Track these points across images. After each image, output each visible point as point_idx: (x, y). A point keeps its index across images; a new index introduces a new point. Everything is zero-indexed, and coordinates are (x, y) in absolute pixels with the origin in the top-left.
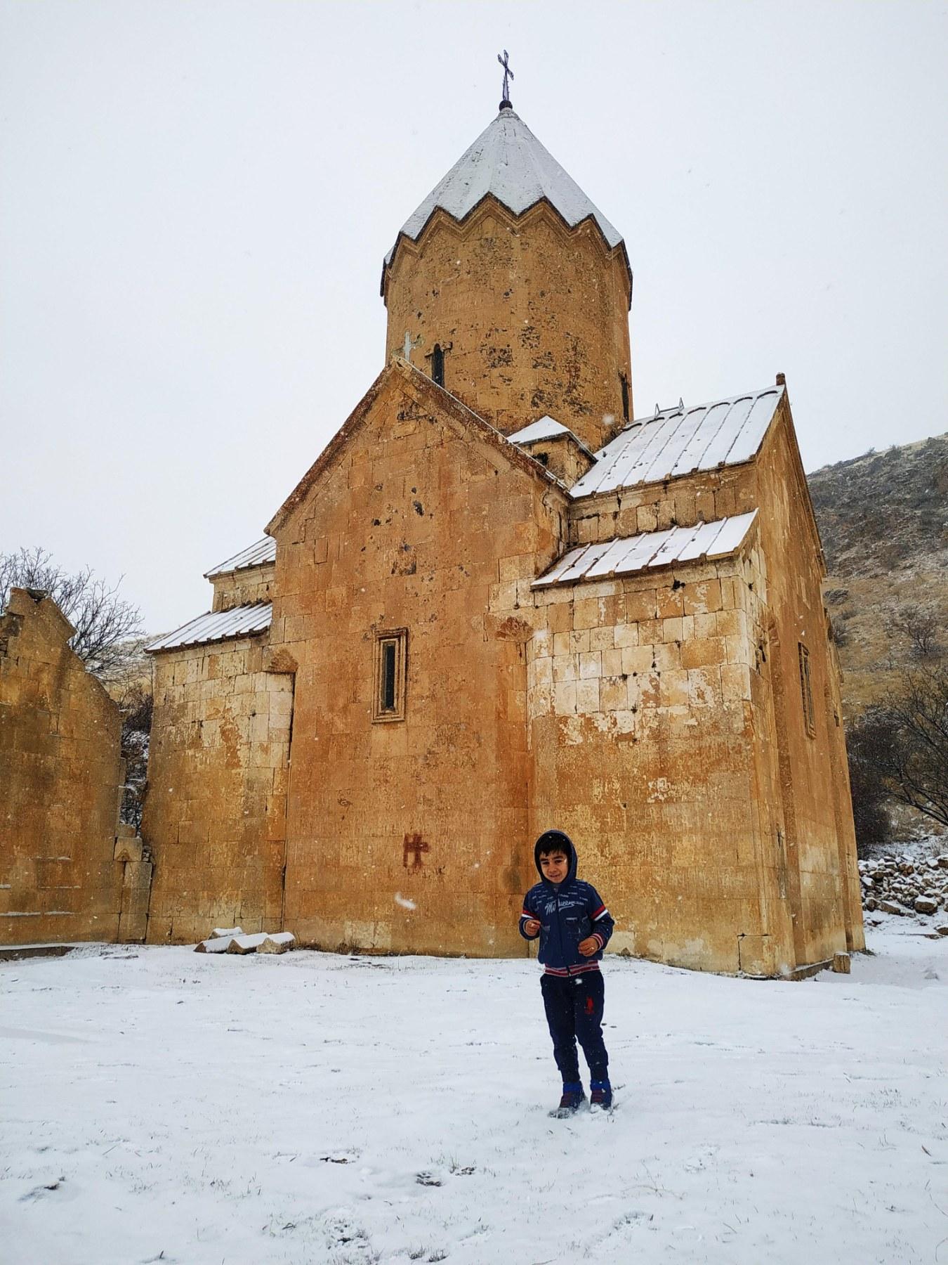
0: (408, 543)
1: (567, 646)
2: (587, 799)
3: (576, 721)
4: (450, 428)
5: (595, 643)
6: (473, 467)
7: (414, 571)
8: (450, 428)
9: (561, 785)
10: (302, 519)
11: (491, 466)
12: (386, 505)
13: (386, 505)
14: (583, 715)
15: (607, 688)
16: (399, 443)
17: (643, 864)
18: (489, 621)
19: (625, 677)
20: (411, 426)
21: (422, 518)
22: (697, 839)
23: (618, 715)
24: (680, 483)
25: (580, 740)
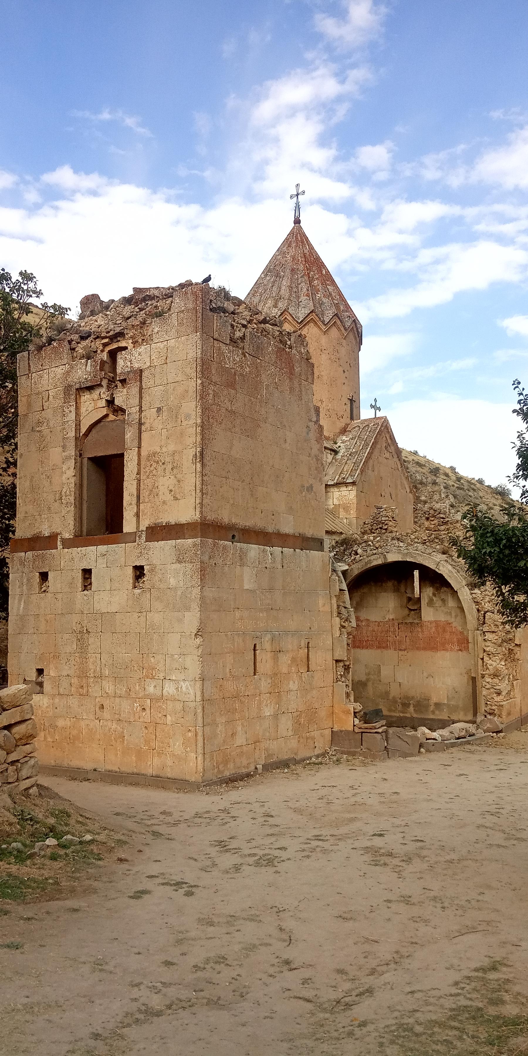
20: (387, 455)
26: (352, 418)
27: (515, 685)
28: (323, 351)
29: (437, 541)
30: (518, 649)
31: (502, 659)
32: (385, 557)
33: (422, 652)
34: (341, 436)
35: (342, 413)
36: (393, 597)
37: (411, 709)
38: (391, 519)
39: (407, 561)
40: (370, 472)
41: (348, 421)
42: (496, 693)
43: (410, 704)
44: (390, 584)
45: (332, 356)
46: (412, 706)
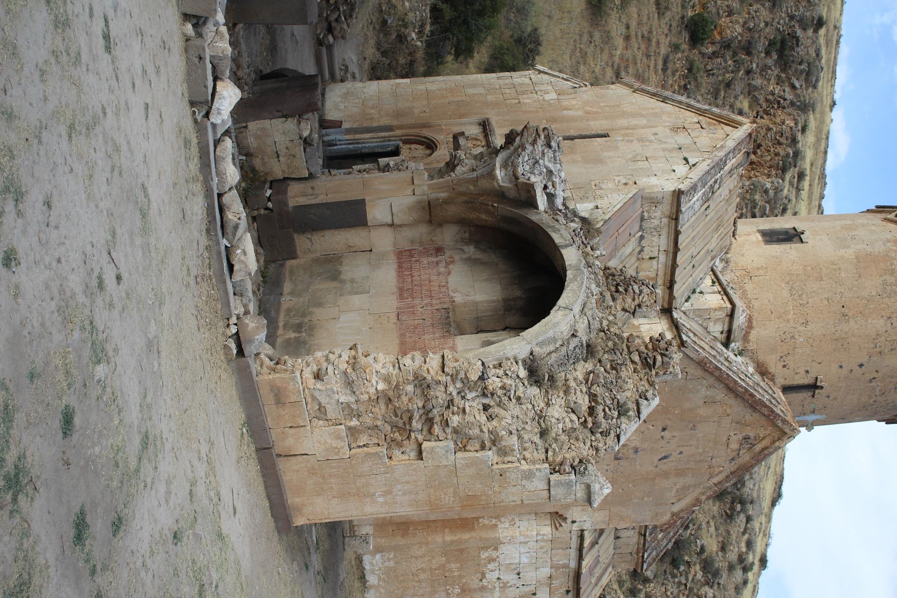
1: (542, 548)
2: (448, 562)
3: (494, 554)
4: (720, 472)
5: (541, 560)
6: (685, 488)
7: (616, 459)
8: (720, 472)
9: (457, 550)
10: (686, 370)
11: (679, 500)
12: (675, 434)
13: (675, 434)
14: (498, 557)
15: (513, 567)
16: (725, 438)
17: (414, 586)
18: (568, 507)
19: (518, 574)
20: (734, 446)
21: (656, 460)
23: (497, 572)
24: (642, 541)
25: (483, 557)
26: (786, 389)
27: (340, 427)
28: (889, 321)
29: (610, 344)
30: (413, 455)
31: (389, 383)
32: (567, 246)
33: (397, 341)
34: (752, 365)
35: (791, 365)
36: (495, 298)
38: (637, 302)
39: (565, 271)
41: (780, 381)
42: (319, 370)
43: (300, 332)
44: (518, 293)
45: (883, 338)
46: (297, 335)
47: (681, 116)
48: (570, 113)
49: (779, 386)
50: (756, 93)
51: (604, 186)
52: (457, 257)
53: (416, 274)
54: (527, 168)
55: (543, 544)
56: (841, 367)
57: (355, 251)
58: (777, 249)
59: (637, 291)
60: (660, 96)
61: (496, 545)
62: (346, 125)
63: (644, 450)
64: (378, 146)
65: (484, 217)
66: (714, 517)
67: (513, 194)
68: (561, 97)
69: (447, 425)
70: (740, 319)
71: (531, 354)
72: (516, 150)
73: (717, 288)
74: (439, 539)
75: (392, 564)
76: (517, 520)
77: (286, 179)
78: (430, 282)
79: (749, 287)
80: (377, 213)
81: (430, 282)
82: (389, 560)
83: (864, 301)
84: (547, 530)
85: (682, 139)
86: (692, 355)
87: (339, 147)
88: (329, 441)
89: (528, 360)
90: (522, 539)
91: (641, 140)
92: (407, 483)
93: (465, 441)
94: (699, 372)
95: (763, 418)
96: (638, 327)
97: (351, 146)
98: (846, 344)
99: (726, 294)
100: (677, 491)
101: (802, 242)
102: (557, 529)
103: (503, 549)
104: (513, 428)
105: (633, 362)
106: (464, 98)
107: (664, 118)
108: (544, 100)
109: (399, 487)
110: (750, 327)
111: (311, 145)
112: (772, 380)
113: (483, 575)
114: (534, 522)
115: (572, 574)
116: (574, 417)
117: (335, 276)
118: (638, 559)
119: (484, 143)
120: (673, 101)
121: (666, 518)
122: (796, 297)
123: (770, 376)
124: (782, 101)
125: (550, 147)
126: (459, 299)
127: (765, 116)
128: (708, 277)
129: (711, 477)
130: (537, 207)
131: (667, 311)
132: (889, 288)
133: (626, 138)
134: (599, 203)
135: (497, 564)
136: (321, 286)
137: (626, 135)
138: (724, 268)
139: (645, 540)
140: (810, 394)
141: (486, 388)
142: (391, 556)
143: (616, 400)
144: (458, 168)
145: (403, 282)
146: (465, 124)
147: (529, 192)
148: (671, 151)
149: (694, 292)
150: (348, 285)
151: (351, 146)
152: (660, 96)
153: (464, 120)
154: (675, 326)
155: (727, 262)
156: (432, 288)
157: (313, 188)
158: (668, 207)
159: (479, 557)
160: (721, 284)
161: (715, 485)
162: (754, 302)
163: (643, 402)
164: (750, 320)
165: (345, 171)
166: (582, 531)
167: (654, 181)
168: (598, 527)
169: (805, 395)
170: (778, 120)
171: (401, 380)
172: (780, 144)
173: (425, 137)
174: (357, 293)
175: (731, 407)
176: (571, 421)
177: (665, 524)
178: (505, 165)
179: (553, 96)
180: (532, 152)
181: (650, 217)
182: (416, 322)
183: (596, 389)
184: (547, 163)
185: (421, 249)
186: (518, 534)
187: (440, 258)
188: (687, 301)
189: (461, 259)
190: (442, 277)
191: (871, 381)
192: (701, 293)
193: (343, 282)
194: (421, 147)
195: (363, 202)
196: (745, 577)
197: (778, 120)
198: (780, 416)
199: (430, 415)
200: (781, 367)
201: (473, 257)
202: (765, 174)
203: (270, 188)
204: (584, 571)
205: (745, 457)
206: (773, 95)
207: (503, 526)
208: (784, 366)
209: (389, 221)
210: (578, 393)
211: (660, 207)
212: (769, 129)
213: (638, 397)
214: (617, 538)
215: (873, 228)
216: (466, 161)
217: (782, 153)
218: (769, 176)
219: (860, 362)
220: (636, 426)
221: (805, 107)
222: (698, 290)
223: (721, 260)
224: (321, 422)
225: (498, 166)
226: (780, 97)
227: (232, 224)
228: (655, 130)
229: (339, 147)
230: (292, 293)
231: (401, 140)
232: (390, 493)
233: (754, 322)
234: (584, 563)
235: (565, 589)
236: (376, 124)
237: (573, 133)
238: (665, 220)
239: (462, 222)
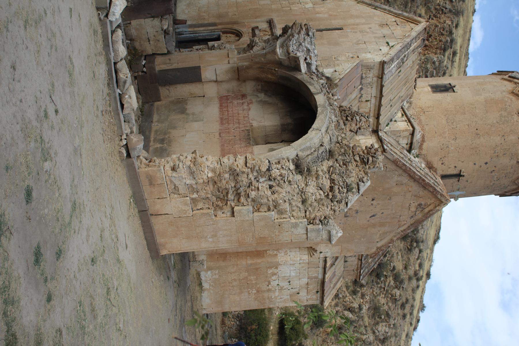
0: (359, 214)
1: (303, 267)
3: (276, 271)
4: (405, 224)
5: (302, 274)
6: (385, 233)
7: (346, 216)
8: (405, 224)
10: (386, 166)
11: (381, 240)
15: (286, 278)
16: (408, 205)
17: (230, 289)
18: (317, 244)
19: (289, 282)
20: (413, 209)
22: (238, 299)
23: (277, 281)
24: (360, 264)
25: (269, 272)
26: (443, 177)
28: (503, 138)
29: (343, 150)
30: (229, 214)
31: (215, 173)
32: (318, 93)
34: (424, 163)
35: (446, 163)
36: (276, 124)
37: (159, 145)
38: (358, 126)
40: (396, 178)
41: (440, 172)
43: (163, 144)
44: (289, 121)
46: (161, 145)
47: (385, 18)
48: (321, 15)
49: (439, 175)
50: (429, 5)
51: (340, 59)
52: (254, 100)
53: (230, 110)
54: (295, 48)
55: (303, 265)
56: (475, 164)
57: (194, 96)
58: (439, 96)
59: (358, 120)
60: (373, 6)
61: (276, 266)
62: (189, 23)
63: (361, 211)
64: (208, 35)
65: (270, 76)
66: (401, 250)
67: (286, 63)
68: (315, 6)
69: (249, 197)
70: (418, 136)
71: (297, 156)
72: (289, 37)
73: (405, 118)
74: (244, 263)
75: (217, 276)
76: (288, 251)
77: (154, 54)
78: (238, 114)
79: (423, 118)
80: (207, 74)
81: (238, 114)
82: (215, 274)
83: (489, 126)
84: (306, 257)
85: (386, 31)
86: (389, 157)
87: (185, 35)
88: (180, 206)
89: (295, 160)
90: (292, 262)
91: (361, 32)
92: (225, 230)
93: (259, 206)
94: (393, 167)
95: (430, 193)
96: (359, 141)
97: (192, 35)
98: (478, 151)
99: (410, 122)
100: (380, 235)
101: (454, 92)
102: (311, 256)
103: (280, 268)
104: (286, 199)
105: (355, 161)
106: (258, 7)
107: (376, 18)
108: (305, 8)
109: (221, 232)
110: (423, 141)
111: (168, 34)
112: (435, 172)
113: (269, 283)
114: (298, 253)
115: (320, 282)
116: (322, 193)
117: (183, 111)
118: (357, 273)
119: (270, 33)
120: (381, 8)
121: (374, 250)
122: (450, 124)
123: (434, 169)
124: (444, 10)
125: (308, 35)
126: (255, 124)
127: (434, 18)
128: (400, 112)
129: (399, 227)
130: (300, 71)
131: (376, 132)
132: (503, 119)
133: (353, 31)
134: (337, 68)
135: (277, 277)
136: (175, 117)
137: (353, 29)
138: (409, 107)
139: (361, 262)
140: (457, 179)
141: (271, 176)
142: (217, 272)
143: (345, 183)
144: (255, 48)
145: (223, 115)
146: (259, 22)
147: (296, 61)
148: (379, 38)
149: (391, 120)
150: (191, 117)
151: (192, 35)
152: (373, 6)
153: (258, 20)
154: (380, 140)
155: (410, 103)
156: (240, 118)
157: (170, 60)
158: (377, 71)
159: (267, 272)
160: (407, 116)
161: (402, 231)
162: (425, 127)
163: (361, 184)
164: (423, 137)
165: (188, 49)
166: (326, 257)
167: (369, 56)
168: (335, 256)
169: (455, 180)
170: (442, 21)
171: (222, 171)
172: (442, 35)
173: (235, 30)
174: (196, 121)
175: (411, 187)
176: (320, 194)
177: (373, 254)
178: (282, 46)
179: (310, 5)
180: (298, 38)
181: (366, 77)
182: (230, 138)
183: (334, 176)
184: (306, 45)
185: (233, 95)
186: (289, 260)
187: (244, 100)
188: (387, 126)
189: (257, 101)
190: (245, 112)
191: (491, 172)
192: (395, 121)
193: (188, 114)
194: (233, 35)
195: (199, 68)
196: (418, 284)
197: (442, 21)
198: (439, 192)
199: (239, 191)
200: (440, 164)
201: (264, 100)
202: (433, 53)
203: (145, 60)
204: (326, 280)
205: (419, 216)
206: (439, 5)
207: (281, 255)
208: (442, 164)
209: (215, 79)
210: (324, 178)
211: (372, 71)
212: (436, 26)
213: (358, 181)
214: (345, 261)
215: (495, 84)
216: (259, 44)
217: (444, 40)
218: (436, 54)
219: (485, 161)
220: (357, 197)
221: (458, 13)
222: (393, 120)
223: (407, 102)
224: (176, 196)
225: (278, 46)
226: (443, 7)
227: (122, 80)
228: (369, 26)
229: (185, 35)
230: (158, 121)
231: (221, 31)
232: (216, 236)
233: (426, 138)
234: (327, 276)
235: (315, 290)
236: (206, 22)
237: (322, 27)
238: (375, 79)
239: (257, 79)
